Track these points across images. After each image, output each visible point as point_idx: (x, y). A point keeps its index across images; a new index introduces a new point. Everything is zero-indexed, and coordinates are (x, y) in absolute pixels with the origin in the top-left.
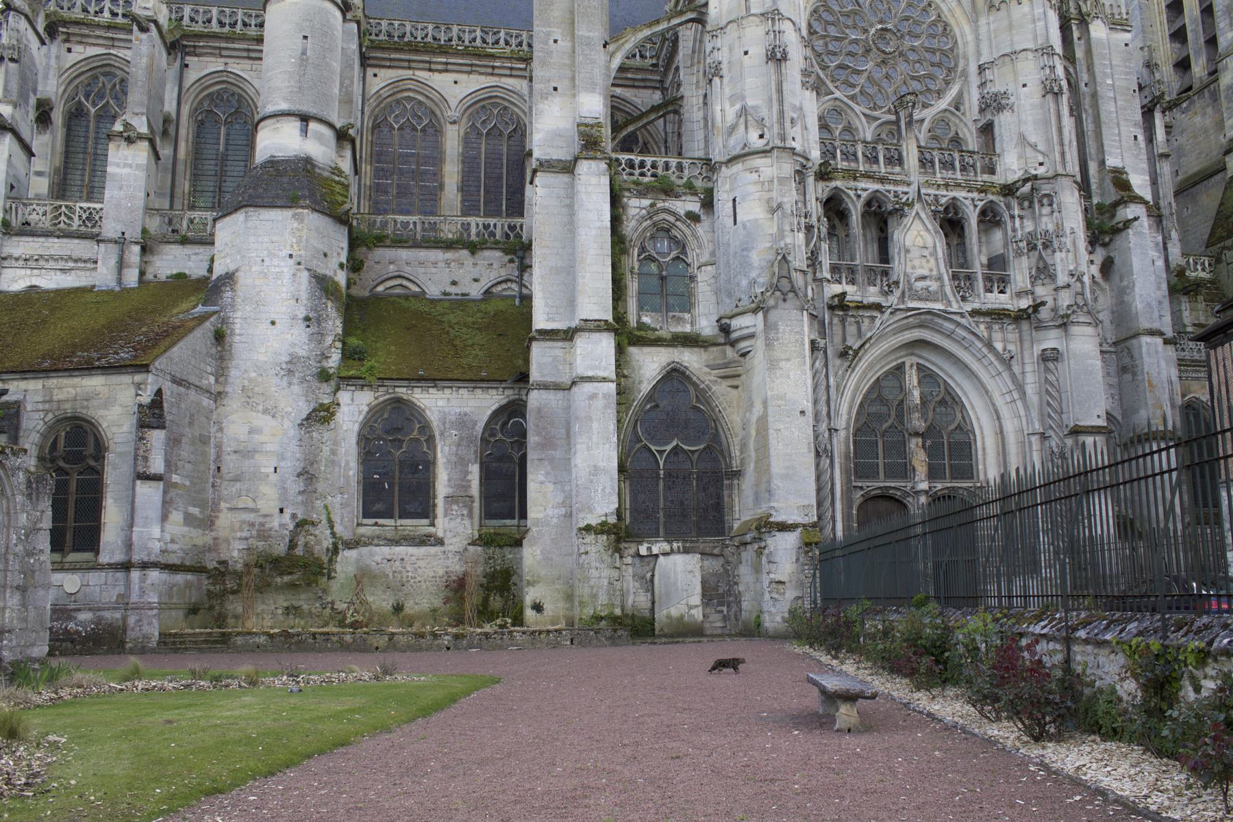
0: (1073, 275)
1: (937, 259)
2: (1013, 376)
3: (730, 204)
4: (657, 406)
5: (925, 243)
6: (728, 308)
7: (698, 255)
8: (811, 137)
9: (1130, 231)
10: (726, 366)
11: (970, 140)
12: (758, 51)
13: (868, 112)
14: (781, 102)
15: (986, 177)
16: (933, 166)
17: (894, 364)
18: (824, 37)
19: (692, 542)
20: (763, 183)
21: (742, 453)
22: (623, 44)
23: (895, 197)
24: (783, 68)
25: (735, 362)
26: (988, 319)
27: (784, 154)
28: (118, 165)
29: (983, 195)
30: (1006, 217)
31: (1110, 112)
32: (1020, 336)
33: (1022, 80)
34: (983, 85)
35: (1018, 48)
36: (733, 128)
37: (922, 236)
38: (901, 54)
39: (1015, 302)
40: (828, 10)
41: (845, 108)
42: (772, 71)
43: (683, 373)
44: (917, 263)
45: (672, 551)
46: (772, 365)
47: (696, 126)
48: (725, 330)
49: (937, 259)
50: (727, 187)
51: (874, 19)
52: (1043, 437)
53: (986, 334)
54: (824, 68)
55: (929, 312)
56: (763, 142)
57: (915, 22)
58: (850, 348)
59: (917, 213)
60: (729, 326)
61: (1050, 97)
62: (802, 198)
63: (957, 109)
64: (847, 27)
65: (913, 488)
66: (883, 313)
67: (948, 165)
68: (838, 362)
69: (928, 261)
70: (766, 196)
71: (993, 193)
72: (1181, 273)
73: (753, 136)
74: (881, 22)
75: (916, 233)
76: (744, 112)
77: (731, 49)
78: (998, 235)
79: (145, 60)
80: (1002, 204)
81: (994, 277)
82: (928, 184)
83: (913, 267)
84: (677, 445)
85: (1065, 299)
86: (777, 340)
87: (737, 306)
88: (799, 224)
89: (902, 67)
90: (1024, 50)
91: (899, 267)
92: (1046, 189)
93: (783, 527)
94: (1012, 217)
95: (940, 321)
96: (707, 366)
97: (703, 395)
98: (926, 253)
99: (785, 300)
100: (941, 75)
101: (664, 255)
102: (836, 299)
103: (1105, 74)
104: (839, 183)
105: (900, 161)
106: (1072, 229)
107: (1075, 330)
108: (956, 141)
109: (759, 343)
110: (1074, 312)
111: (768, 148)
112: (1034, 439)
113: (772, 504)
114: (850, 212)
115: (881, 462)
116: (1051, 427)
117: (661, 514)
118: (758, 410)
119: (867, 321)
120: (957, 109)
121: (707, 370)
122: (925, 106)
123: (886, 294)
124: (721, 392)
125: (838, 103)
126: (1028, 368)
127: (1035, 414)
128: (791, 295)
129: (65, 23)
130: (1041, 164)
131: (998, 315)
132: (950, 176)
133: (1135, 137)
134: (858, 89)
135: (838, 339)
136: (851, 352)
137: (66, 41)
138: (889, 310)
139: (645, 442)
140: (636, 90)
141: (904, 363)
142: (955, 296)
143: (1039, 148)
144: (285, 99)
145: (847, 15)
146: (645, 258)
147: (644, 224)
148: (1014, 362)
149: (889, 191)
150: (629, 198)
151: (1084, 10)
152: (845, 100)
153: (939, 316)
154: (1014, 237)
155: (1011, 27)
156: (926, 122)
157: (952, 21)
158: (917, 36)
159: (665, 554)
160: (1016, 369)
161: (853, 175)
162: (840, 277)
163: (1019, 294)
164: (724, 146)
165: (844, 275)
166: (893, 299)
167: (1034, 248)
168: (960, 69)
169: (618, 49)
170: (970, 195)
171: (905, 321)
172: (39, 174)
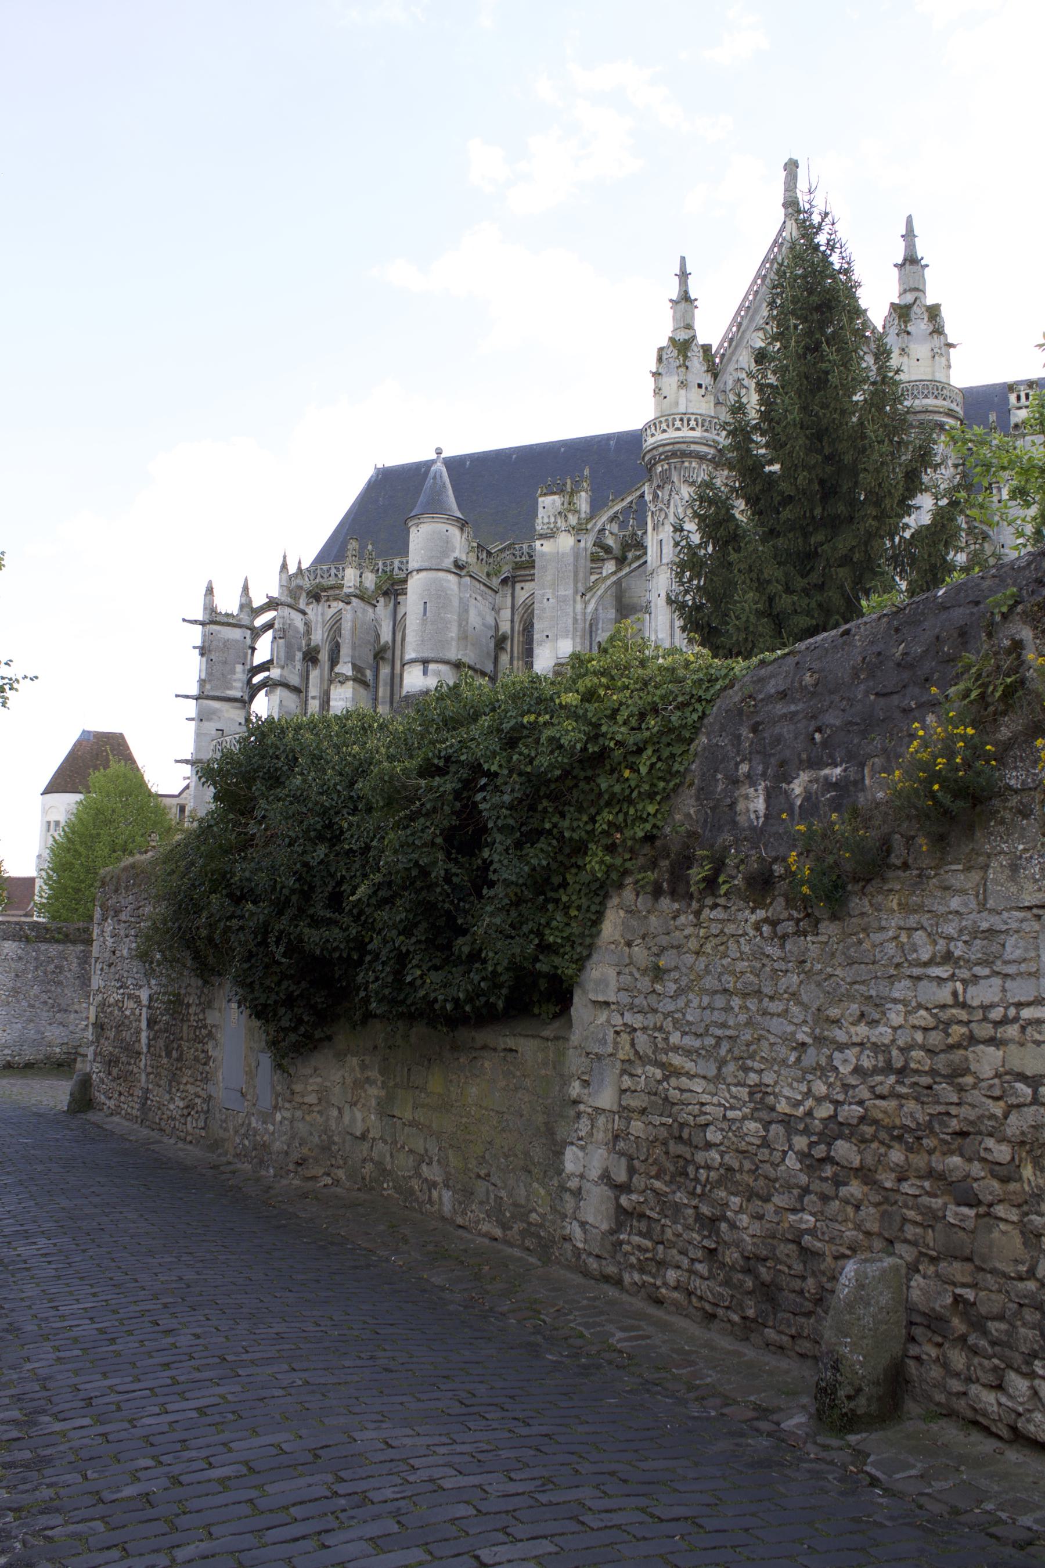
28: (336, 700)
79: (349, 624)
129: (325, 589)
137: (328, 600)
144: (414, 650)
169: (592, 597)
172: (313, 698)
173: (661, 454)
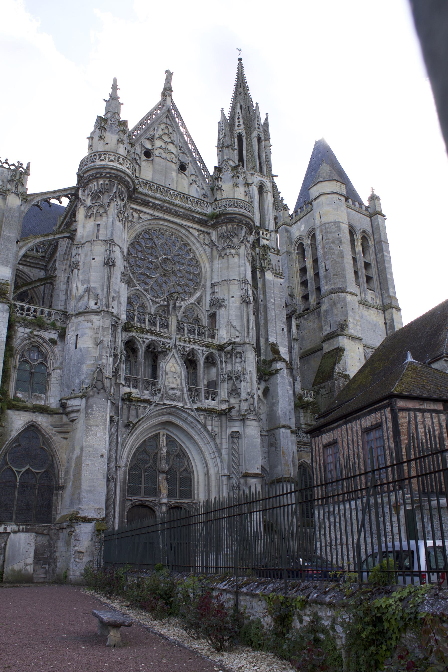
0: (249, 394)
1: (181, 379)
2: (216, 444)
3: (75, 338)
4: (20, 445)
5: (176, 370)
6: (66, 394)
7: (53, 363)
8: (122, 308)
9: (278, 375)
10: (61, 426)
11: (204, 320)
12: (100, 259)
13: (153, 299)
14: (109, 287)
15: (210, 340)
16: (184, 331)
17: (154, 433)
18: (135, 257)
19: (31, 526)
20: (94, 329)
21: (65, 476)
22: (27, 243)
23: (163, 344)
24: (112, 270)
25: (67, 424)
26: (205, 414)
27: (107, 315)
30: (219, 362)
31: (272, 315)
32: (221, 424)
33: (232, 294)
34: (212, 293)
35: (231, 278)
36: (81, 297)
38: (173, 272)
39: (219, 405)
40: (139, 244)
41: (142, 295)
42: (106, 271)
43: (37, 428)
44: (171, 380)
45: (19, 531)
46: (88, 428)
47: (61, 293)
48: (64, 406)
49: (181, 379)
50: (74, 328)
51: (162, 253)
52: (229, 478)
53: (203, 421)
54: (133, 273)
55: (175, 407)
56: (96, 307)
57: (182, 258)
58: (131, 422)
59: (173, 354)
60: (66, 404)
61: (244, 304)
62: (114, 339)
63: (199, 304)
64: (148, 254)
65: (159, 501)
66: (150, 405)
67: (191, 331)
68: (124, 429)
69: (177, 380)
70: (95, 336)
71: (213, 349)
72: (300, 398)
73: (92, 303)
74: (165, 255)
75: (171, 365)
76: (88, 290)
77: (86, 256)
78: (213, 371)
80: (217, 355)
81: (210, 392)
82: (180, 340)
83: (169, 383)
84: (29, 469)
85: (245, 407)
86: (92, 414)
87: (72, 394)
88: (110, 353)
89: (173, 278)
90: (234, 280)
91: (161, 381)
92: (239, 349)
93: (85, 520)
94: (221, 362)
95: (180, 412)
96: (51, 425)
97: (47, 441)
98: (176, 375)
99: (98, 393)
100: (192, 285)
101: (34, 360)
102: (126, 396)
103: (271, 297)
104: (134, 334)
105: (167, 326)
106: (250, 371)
107: (248, 422)
108: (197, 320)
109: (82, 415)
110: (248, 413)
111: (98, 310)
112: (225, 479)
113: (80, 507)
114: (138, 350)
115: (142, 486)
116: (233, 473)
117: (15, 509)
118: (77, 452)
119: (141, 409)
120: (199, 304)
121: (51, 427)
122: (183, 300)
123: (153, 395)
124: (57, 439)
125: (138, 292)
126: (224, 441)
127: (225, 465)
128: (102, 391)
130: (238, 337)
131: (210, 412)
132: (192, 337)
133: (283, 329)
134: (149, 287)
135: (125, 417)
136: (131, 425)
138: (154, 404)
139: (10, 465)
140: (31, 268)
141: (159, 433)
142: (189, 400)
143: (237, 328)
145: (148, 248)
146: (23, 361)
147: (25, 342)
148: (217, 437)
149: (160, 341)
150: (19, 327)
151: (263, 265)
152: (142, 291)
153: (180, 409)
155: (228, 267)
156: (183, 308)
157: (200, 260)
158: (183, 265)
159: (15, 532)
160: (218, 441)
161: (142, 331)
162: (130, 384)
163: (222, 402)
164: (75, 306)
165: (132, 383)
166: (157, 399)
167: (231, 379)
168: (202, 284)
170: (201, 348)
171: (162, 411)
173: (107, 173)
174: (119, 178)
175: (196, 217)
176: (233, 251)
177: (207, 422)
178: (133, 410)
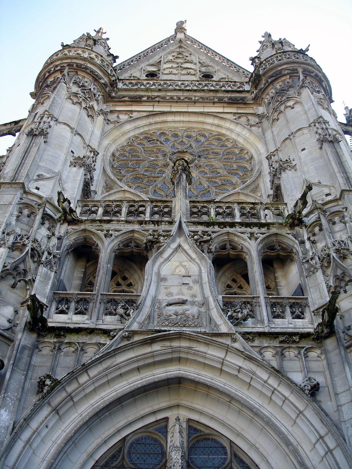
17: (151, 419)
29: (266, 229)
35: (294, 131)
37: (184, 267)
61: (326, 146)
80: (290, 236)
83: (170, 294)
94: (302, 242)
95: (202, 348)
136: (48, 382)
142: (221, 316)
148: (322, 396)
154: (304, 258)
171: (147, 350)
173: (57, 66)
174: (75, 66)
175: (224, 98)
176: (290, 103)
177: (287, 365)
178: (67, 355)
